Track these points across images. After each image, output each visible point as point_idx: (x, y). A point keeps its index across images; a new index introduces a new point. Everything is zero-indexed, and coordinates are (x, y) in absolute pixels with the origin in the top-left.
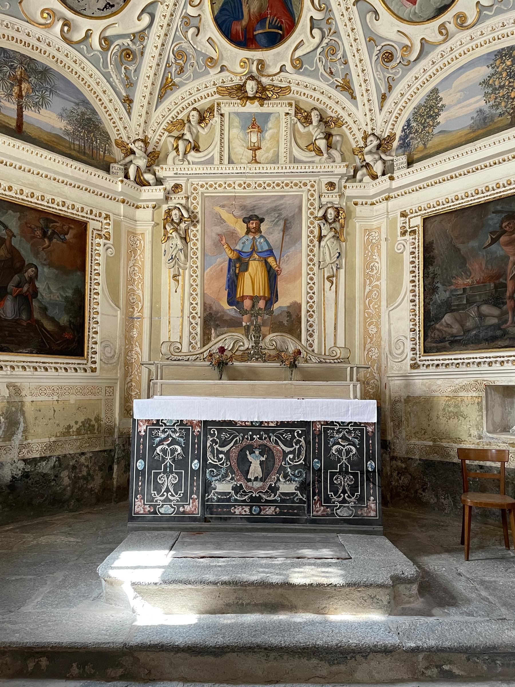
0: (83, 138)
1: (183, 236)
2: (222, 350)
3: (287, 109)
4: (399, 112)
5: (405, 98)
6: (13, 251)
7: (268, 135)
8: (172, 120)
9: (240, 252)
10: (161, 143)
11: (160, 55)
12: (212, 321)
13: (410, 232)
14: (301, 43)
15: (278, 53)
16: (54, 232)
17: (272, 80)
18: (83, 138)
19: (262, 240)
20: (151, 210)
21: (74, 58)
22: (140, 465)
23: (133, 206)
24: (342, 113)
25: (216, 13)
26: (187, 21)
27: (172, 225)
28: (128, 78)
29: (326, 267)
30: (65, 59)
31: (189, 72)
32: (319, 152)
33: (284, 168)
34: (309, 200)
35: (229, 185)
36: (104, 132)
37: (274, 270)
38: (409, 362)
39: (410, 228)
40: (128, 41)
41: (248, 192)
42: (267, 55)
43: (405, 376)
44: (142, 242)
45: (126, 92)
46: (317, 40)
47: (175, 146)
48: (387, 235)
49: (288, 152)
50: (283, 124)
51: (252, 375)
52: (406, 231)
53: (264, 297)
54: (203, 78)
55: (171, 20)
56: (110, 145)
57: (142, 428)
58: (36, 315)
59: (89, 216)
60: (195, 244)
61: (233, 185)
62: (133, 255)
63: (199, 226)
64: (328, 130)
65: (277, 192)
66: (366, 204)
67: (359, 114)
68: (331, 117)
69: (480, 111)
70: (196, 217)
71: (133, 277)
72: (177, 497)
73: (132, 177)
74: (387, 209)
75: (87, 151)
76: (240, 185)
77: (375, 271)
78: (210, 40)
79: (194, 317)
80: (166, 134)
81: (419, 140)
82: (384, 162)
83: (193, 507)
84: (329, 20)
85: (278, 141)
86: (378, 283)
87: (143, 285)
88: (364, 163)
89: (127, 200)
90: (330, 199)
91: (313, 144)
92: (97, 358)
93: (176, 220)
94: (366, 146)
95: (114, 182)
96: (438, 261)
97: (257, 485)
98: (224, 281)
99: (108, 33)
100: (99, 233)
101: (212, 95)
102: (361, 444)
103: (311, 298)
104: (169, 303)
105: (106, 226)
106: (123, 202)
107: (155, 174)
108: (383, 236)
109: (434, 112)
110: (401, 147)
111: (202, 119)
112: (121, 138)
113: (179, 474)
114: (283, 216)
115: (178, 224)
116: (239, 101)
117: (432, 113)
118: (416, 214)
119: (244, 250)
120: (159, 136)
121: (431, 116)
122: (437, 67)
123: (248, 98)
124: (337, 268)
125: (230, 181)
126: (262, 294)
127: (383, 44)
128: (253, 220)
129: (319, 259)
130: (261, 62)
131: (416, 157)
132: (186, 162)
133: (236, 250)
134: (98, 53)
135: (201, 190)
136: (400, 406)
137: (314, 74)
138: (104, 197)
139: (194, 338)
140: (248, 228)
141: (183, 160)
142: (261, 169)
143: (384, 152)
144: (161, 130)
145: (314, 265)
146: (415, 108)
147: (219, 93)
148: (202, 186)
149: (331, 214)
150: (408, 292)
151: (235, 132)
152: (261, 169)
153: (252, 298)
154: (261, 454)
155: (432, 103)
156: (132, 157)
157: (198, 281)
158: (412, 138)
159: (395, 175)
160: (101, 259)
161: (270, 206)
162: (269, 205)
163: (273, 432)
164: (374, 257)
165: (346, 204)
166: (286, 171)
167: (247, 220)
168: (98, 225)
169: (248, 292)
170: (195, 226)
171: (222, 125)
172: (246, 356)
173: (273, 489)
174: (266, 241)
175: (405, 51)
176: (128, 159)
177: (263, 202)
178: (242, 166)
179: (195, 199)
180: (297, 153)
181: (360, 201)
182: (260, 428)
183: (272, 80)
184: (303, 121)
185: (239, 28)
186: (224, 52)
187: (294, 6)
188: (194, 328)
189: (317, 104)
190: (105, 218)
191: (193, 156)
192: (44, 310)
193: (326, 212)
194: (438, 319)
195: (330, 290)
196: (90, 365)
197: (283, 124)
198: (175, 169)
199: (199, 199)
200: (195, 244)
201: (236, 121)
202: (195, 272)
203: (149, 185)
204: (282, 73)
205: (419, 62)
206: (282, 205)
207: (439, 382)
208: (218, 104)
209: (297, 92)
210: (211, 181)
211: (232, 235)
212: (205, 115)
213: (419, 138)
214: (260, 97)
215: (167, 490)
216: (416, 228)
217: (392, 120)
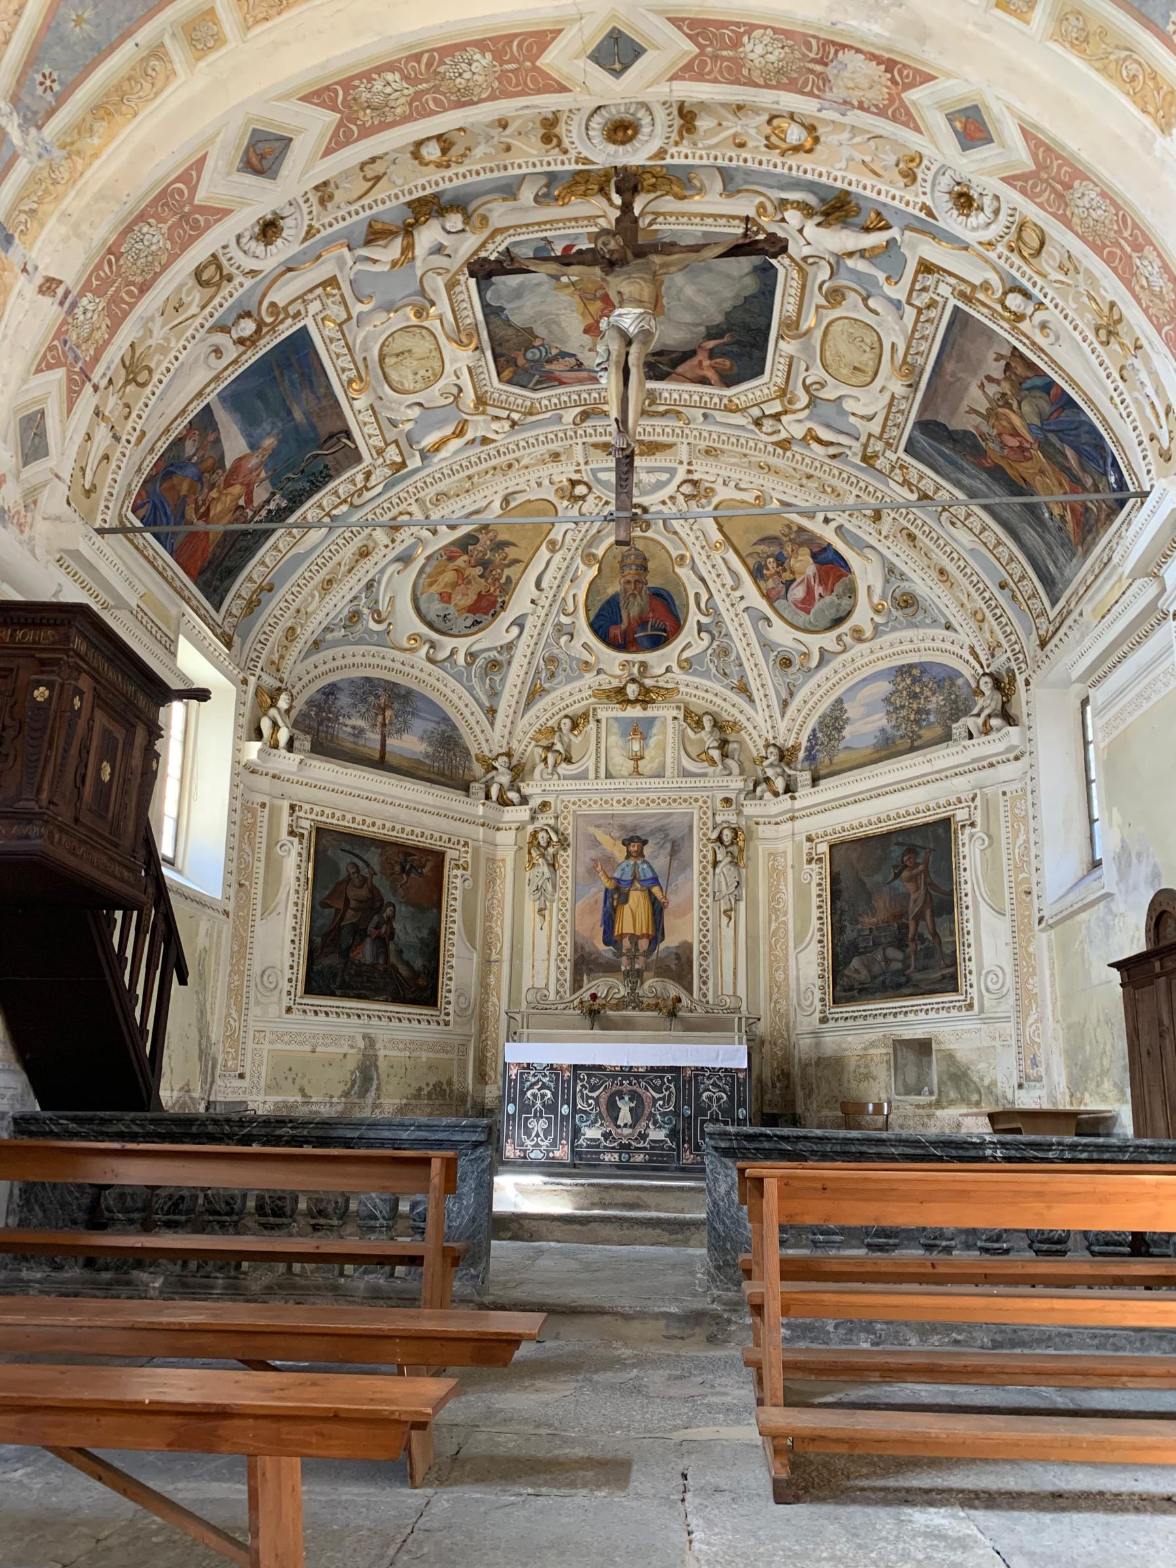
0: (442, 759)
2: (594, 997)
3: (675, 713)
5: (809, 706)
6: (373, 890)
7: (652, 742)
9: (618, 880)
12: (584, 964)
16: (412, 867)
18: (442, 759)
20: (513, 832)
22: (511, 1109)
26: (559, 629)
28: (492, 688)
30: (427, 678)
31: (561, 677)
32: (713, 762)
35: (606, 802)
38: (817, 1015)
41: (629, 810)
43: (815, 1034)
46: (706, 643)
50: (670, 730)
51: (628, 1024)
53: (647, 936)
56: (470, 761)
57: (513, 1072)
58: (393, 959)
63: (570, 851)
65: (664, 809)
67: (760, 718)
69: (883, 730)
70: (566, 839)
72: (546, 1143)
73: (494, 797)
76: (619, 802)
78: (585, 646)
79: (562, 961)
83: (562, 1153)
90: (726, 818)
91: (706, 753)
92: (451, 1008)
93: (543, 843)
96: (845, 895)
97: (627, 1131)
98: (598, 916)
99: (474, 649)
102: (732, 1091)
103: (704, 936)
107: (519, 791)
108: (790, 863)
111: (575, 726)
113: (549, 1119)
115: (545, 849)
120: (526, 747)
123: (629, 702)
124: (737, 901)
125: (607, 797)
128: (635, 841)
130: (643, 665)
131: (822, 772)
135: (572, 808)
136: (811, 1071)
137: (706, 675)
139: (562, 986)
143: (788, 764)
151: (613, 739)
154: (631, 1100)
155: (837, 713)
156: (494, 773)
157: (568, 917)
160: (458, 894)
161: (654, 826)
162: (653, 824)
163: (643, 1077)
169: (628, 928)
170: (565, 850)
171: (598, 732)
172: (621, 1005)
173: (643, 1136)
176: (489, 776)
181: (761, 820)
182: (628, 1073)
185: (618, 632)
188: (562, 973)
191: (564, 768)
192: (400, 952)
194: (847, 963)
196: (443, 1017)
197: (670, 730)
199: (570, 818)
201: (615, 727)
202: (564, 905)
207: (850, 1039)
211: (609, 860)
213: (819, 756)
215: (537, 1135)
217: (794, 729)
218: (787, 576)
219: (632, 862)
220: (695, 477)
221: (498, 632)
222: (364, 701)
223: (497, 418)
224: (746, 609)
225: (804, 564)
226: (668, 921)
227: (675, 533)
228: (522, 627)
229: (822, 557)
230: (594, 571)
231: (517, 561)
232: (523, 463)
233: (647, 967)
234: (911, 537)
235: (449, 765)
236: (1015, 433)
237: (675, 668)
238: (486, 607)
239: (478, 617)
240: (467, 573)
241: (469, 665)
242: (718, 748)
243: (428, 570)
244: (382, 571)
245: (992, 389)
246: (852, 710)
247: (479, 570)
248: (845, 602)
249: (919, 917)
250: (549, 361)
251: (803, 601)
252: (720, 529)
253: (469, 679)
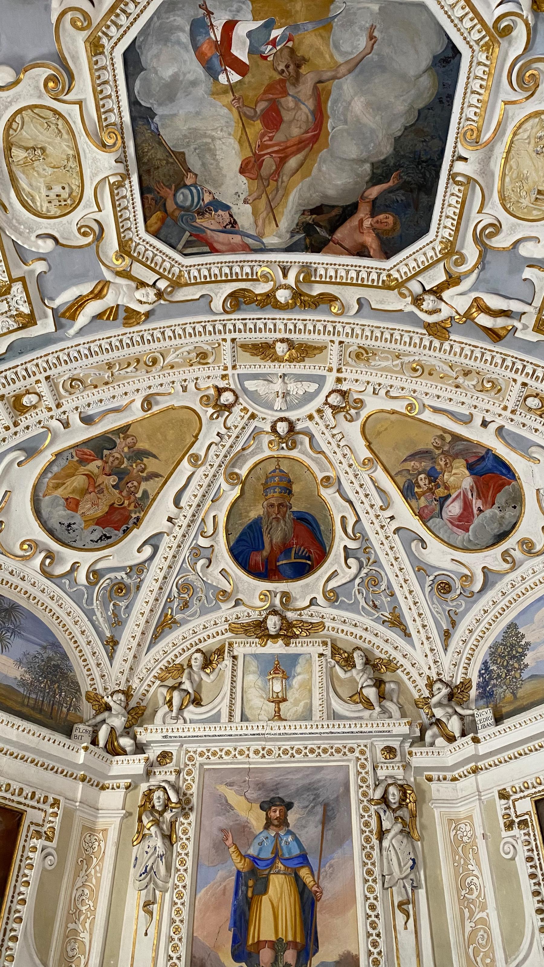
1: (167, 833)
3: (321, 649)
4: (470, 652)
7: (296, 682)
8: (166, 665)
9: (255, 859)
10: (149, 695)
11: (161, 588)
13: (519, 823)
14: (335, 574)
15: (307, 585)
17: (300, 615)
18: (43, 690)
19: (290, 839)
20: (122, 791)
21: (52, 594)
23: (97, 786)
24: (394, 654)
25: (232, 544)
26: (197, 552)
27: (152, 815)
28: (115, 615)
29: (395, 885)
31: (195, 607)
33: (320, 727)
34: (359, 773)
35: (241, 753)
36: (72, 682)
37: (310, 891)
39: (517, 817)
40: (123, 574)
42: (293, 587)
44: (102, 844)
45: (111, 632)
46: (354, 570)
47: (168, 699)
48: (484, 829)
49: (325, 705)
50: (316, 668)
52: (512, 822)
53: (294, 944)
54: (212, 614)
55: (178, 552)
59: (28, 802)
60: (183, 847)
61: (247, 752)
62: (85, 867)
63: (192, 817)
64: (377, 675)
65: (312, 762)
66: (445, 779)
67: (417, 655)
68: (380, 658)
70: (188, 801)
71: (79, 906)
73: (102, 743)
74: (477, 786)
75: (45, 708)
76: (256, 752)
77: (476, 893)
78: (223, 572)
80: (158, 683)
81: (505, 687)
82: (462, 717)
84: (367, 548)
85: (310, 691)
86: (483, 915)
87: (92, 923)
88: (434, 720)
89: (89, 776)
90: (390, 772)
91: (360, 693)
94: (433, 696)
95: (75, 750)
99: (99, 566)
100: (38, 829)
101: (223, 634)
103: (375, 944)
104: (133, 958)
105: (50, 819)
106: (83, 780)
107: (135, 738)
108: (479, 831)
109: (517, 652)
110: (482, 698)
111: (207, 663)
112: (95, 689)
114: (321, 799)
115: (161, 814)
116: (257, 640)
117: (514, 652)
118: (522, 794)
119: (261, 856)
120: (147, 686)
121: (514, 657)
122: (509, 598)
125: (242, 745)
126: (290, 938)
127: (436, 574)
128: (276, 804)
129: (382, 871)
130: (286, 595)
131: (504, 710)
132: (181, 721)
133: (249, 856)
134: (83, 588)
135: (199, 760)
137: (354, 607)
138: (56, 772)
140: (268, 818)
141: (177, 718)
142: (287, 728)
143: (460, 705)
144: (151, 678)
145: (374, 881)
146: (490, 647)
147: (232, 631)
148: (201, 755)
149: (394, 795)
150: (537, 932)
151: (251, 678)
152: (287, 728)
153: (273, 945)
156: (106, 714)
157: (185, 915)
158: (495, 685)
159: (480, 735)
160: (32, 875)
161: (301, 783)
162: (299, 781)
164: (470, 866)
165: (415, 779)
166: (322, 731)
167: (266, 806)
168: (38, 816)
170: (186, 816)
171: (233, 670)
174: (296, 840)
175: (465, 581)
176: (99, 718)
177: (290, 777)
178: (260, 724)
179: (189, 773)
180: (338, 706)
183: (300, 615)
184: (343, 663)
185: (259, 559)
186: (240, 585)
187: (324, 536)
189: (360, 643)
190: (52, 806)
191: (191, 712)
193: (386, 792)
195: (406, 928)
197: (316, 668)
198: (164, 730)
199: (196, 773)
200: (183, 847)
201: (253, 666)
202: (180, 896)
203: (125, 753)
204: (312, 607)
205: (486, 593)
206: (319, 781)
208: (230, 644)
209: (333, 628)
210: (214, 747)
211: (242, 830)
212: (212, 659)
214: (285, 635)
216: (527, 817)
218: (441, 492)
221: (127, 551)
223: (142, 284)
224: (397, 531)
226: (322, 920)
227: (322, 452)
228: (156, 549)
229: (478, 468)
232: (170, 359)
237: (321, 600)
238: (117, 522)
239: (107, 531)
240: (99, 481)
241: (92, 584)
242: (374, 685)
243: (55, 469)
247: (112, 480)
248: (509, 513)
250: (201, 213)
251: (460, 518)
252: (369, 447)
253: (90, 601)
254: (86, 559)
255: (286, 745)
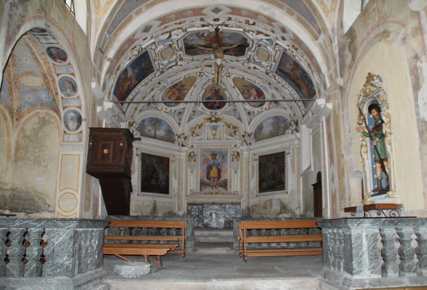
3: (223, 124)
6: (154, 168)
7: (218, 131)
12: (203, 184)
31: (196, 115)
41: (213, 147)
65: (220, 147)
92: (172, 194)
120: (187, 133)
128: (214, 155)
136: (254, 207)
137: (231, 115)
151: (209, 130)
191: (197, 137)
192: (160, 182)
218: (250, 94)
219: (213, 160)
220: (229, 72)
222: (151, 122)
225: (254, 92)
230: (204, 91)
231: (186, 89)
233: (217, 185)
234: (277, 89)
235: (170, 137)
236: (296, 75)
238: (179, 99)
244: (156, 93)
245: (292, 66)
246: (265, 125)
247: (177, 91)
249: (278, 174)
254: (174, 108)
255: (216, 144)
